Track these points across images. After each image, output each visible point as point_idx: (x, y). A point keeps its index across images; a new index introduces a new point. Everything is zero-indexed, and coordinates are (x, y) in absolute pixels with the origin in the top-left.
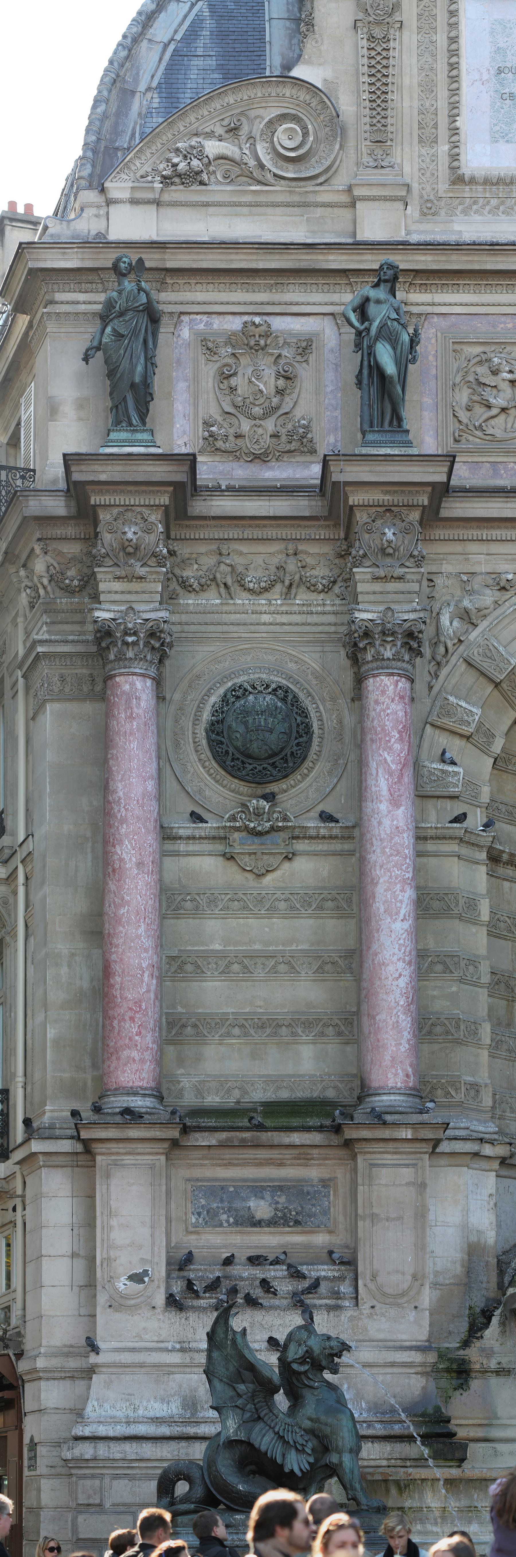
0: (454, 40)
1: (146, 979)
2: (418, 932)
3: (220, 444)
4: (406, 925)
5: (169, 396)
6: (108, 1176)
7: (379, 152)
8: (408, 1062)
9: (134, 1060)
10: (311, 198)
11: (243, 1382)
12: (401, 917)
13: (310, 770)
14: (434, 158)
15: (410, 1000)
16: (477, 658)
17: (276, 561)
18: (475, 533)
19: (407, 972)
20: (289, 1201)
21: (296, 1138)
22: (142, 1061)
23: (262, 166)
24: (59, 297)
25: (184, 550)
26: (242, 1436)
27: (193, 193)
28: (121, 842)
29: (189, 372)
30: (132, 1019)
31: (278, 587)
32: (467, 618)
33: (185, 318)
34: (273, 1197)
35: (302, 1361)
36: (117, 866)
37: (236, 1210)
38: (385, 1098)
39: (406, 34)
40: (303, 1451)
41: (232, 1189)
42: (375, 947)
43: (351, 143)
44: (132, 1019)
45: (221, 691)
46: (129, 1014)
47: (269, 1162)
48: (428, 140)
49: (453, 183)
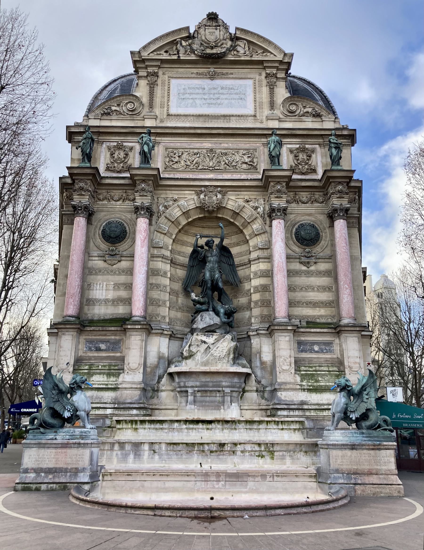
0: (169, 87)
2: (148, 279)
3: (110, 169)
4: (144, 276)
5: (100, 158)
6: (61, 337)
7: (151, 109)
10: (135, 119)
11: (55, 390)
14: (163, 111)
17: (121, 194)
18: (168, 188)
19: (143, 287)
20: (110, 344)
21: (113, 329)
23: (124, 112)
24: (75, 138)
25: (99, 191)
26: (52, 405)
27: (109, 117)
29: (104, 154)
31: (121, 200)
32: (166, 207)
33: (105, 143)
35: (73, 384)
38: (135, 318)
39: (158, 87)
40: (70, 411)
42: (135, 281)
43: (145, 108)
44: (72, 298)
45: (105, 223)
48: (162, 106)
49: (167, 116)
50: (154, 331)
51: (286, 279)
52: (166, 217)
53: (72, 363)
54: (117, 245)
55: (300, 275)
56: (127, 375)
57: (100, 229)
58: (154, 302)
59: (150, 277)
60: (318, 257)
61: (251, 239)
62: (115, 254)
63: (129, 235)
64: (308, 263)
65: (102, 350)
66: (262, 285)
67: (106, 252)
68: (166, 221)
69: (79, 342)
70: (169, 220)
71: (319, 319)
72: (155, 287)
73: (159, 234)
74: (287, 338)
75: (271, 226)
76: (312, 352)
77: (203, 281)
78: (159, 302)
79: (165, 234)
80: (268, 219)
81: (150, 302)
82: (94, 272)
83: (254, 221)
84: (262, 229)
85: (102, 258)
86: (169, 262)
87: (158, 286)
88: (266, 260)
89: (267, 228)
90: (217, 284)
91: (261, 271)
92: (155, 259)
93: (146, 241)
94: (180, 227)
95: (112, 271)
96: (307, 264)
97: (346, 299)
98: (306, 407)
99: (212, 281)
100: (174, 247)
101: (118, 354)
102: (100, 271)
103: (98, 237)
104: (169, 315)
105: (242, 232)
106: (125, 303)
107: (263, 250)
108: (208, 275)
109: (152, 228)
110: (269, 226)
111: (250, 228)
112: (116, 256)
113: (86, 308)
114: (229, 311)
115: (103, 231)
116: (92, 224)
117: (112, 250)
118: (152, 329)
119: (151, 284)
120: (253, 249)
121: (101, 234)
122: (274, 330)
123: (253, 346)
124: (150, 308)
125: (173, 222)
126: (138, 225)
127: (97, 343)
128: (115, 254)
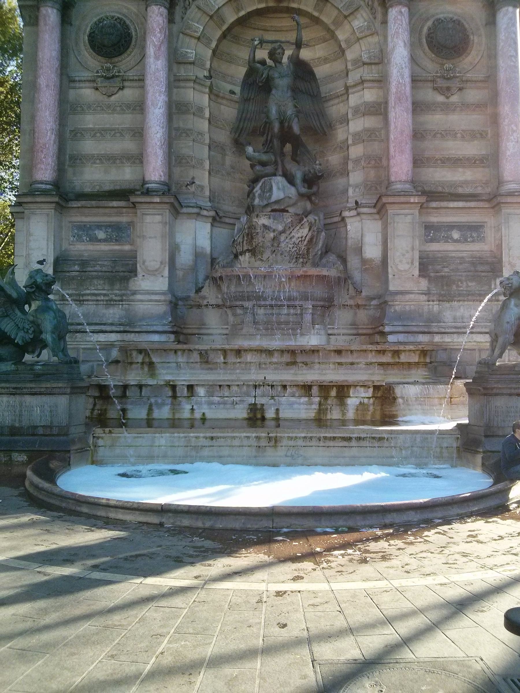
1: (49, 134)
2: (170, 116)
4: (161, 111)
6: (29, 218)
8: (161, 170)
9: (42, 169)
12: (159, 107)
13: (131, 52)
15: (163, 143)
16: (201, 5)
20: (112, 231)
21: (115, 204)
22: (46, 169)
28: (40, 77)
30: (42, 151)
34: (106, 229)
36: (38, 87)
37: (90, 235)
41: (88, 226)
46: (41, 149)
47: (105, 215)
50: (185, 210)
51: (410, 116)
52: (199, 8)
53: (51, 260)
54: (116, 59)
55: (434, 110)
56: (142, 280)
57: (85, 32)
58: (184, 161)
59: (174, 117)
60: (464, 79)
61: (349, 47)
62: (113, 77)
63: (136, 41)
64: (448, 89)
65: (100, 241)
66: (366, 130)
67: (98, 72)
68: (199, 14)
69: (61, 227)
70: (205, 12)
71: (462, 187)
72: (184, 135)
73: (187, 39)
74: (409, 219)
75: (385, 22)
76: (449, 242)
77: (266, 123)
78: (192, 160)
79: (199, 39)
80: (379, 9)
81: (176, 160)
82: (79, 109)
83: (355, 13)
84: (369, 28)
85: (92, 85)
86: (207, 90)
87: (187, 132)
88: (375, 84)
89: (378, 24)
90: (290, 128)
91: (366, 104)
92: (182, 84)
93: (164, 48)
94: (225, 28)
95: (109, 107)
96: (446, 91)
97: (511, 150)
98: (435, 330)
99: (282, 123)
100: (215, 64)
101: (127, 247)
102: (89, 107)
103: (83, 48)
104: (209, 183)
105: (333, 36)
106: (134, 162)
107: (370, 67)
108: (273, 111)
109: (175, 28)
110: (382, 23)
111: (347, 27)
112: (115, 79)
113: (70, 171)
114: (310, 175)
115: (90, 36)
116: (71, 25)
117: (108, 70)
118: (182, 206)
119: (177, 129)
120: (352, 65)
121: (87, 42)
122: (387, 205)
123: (349, 236)
124: (177, 170)
125: (211, 17)
126: (150, 20)
127: (90, 228)
128: (113, 77)
